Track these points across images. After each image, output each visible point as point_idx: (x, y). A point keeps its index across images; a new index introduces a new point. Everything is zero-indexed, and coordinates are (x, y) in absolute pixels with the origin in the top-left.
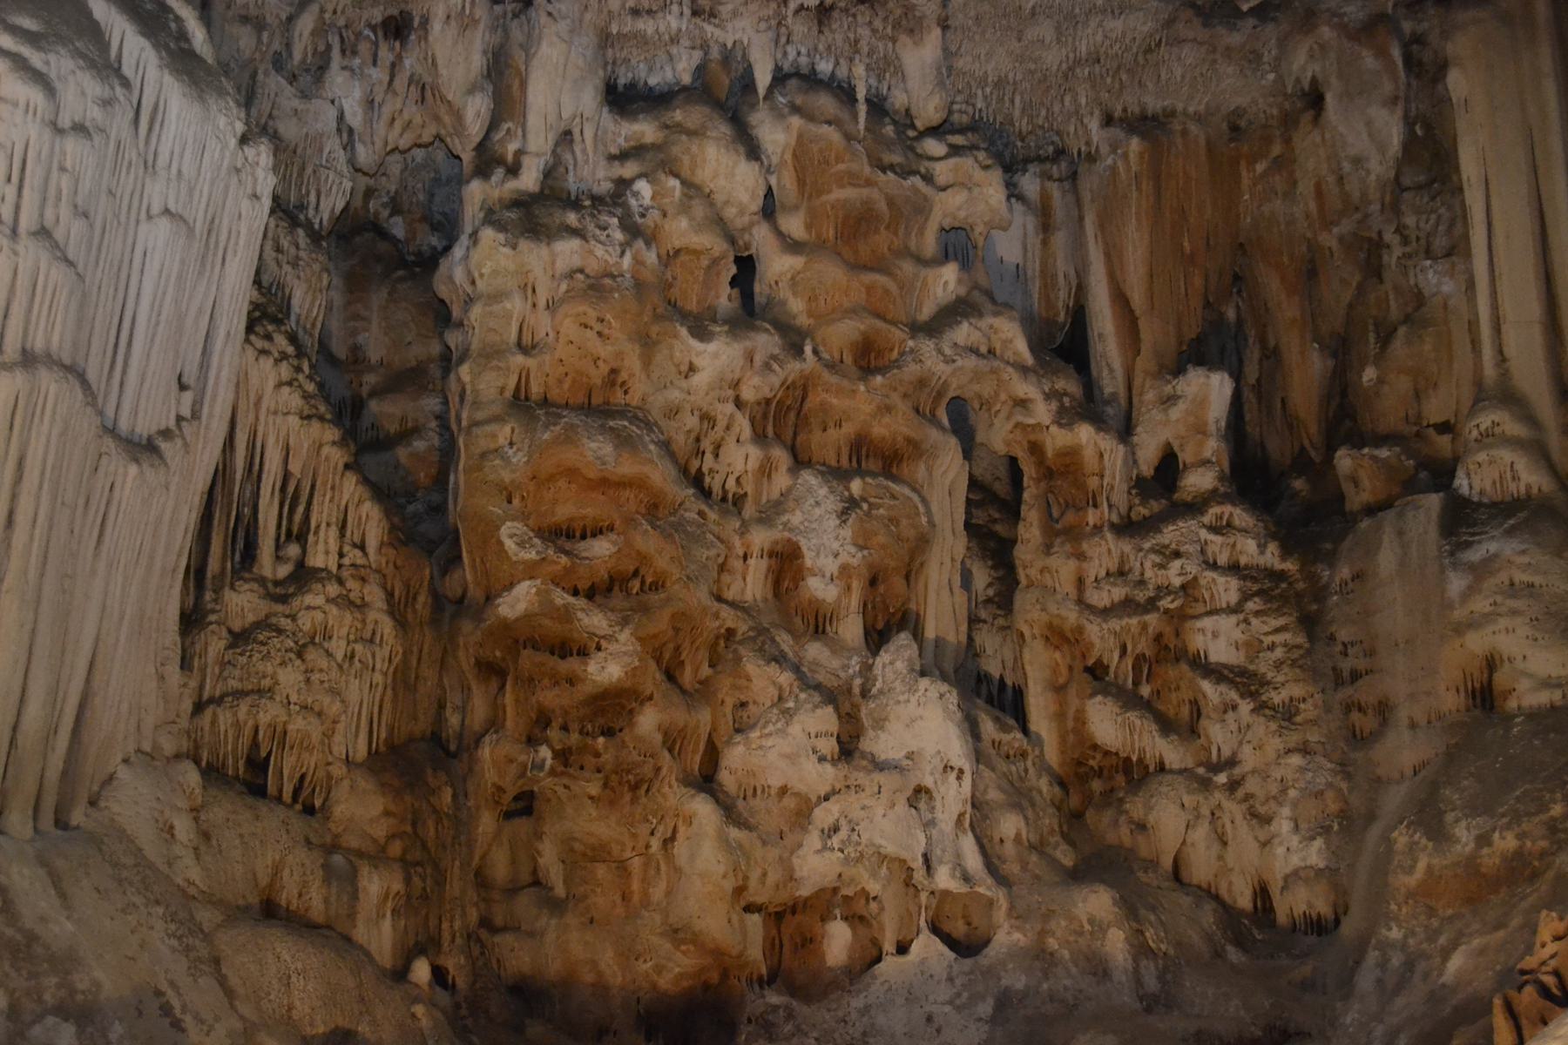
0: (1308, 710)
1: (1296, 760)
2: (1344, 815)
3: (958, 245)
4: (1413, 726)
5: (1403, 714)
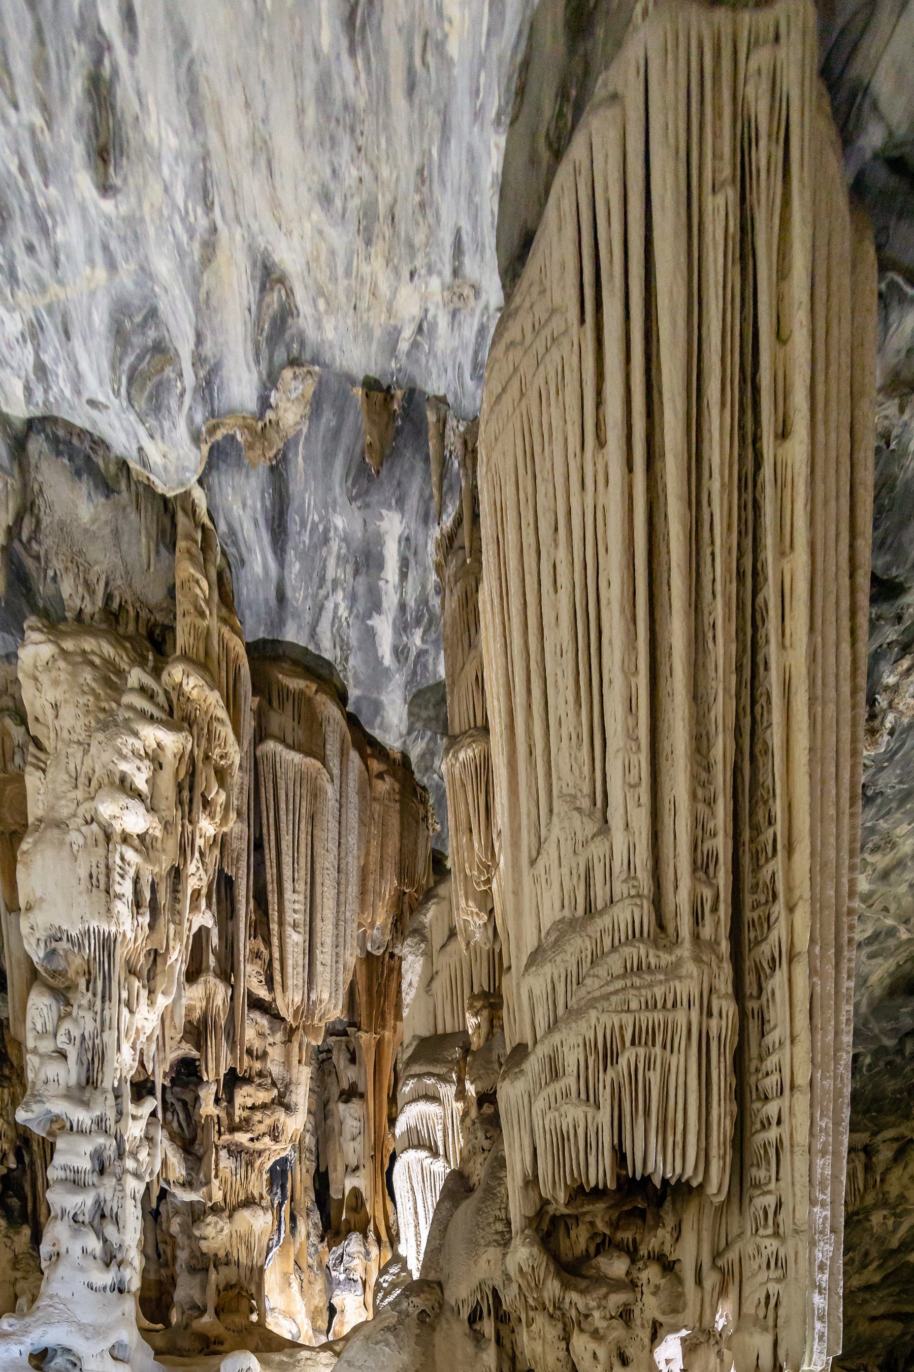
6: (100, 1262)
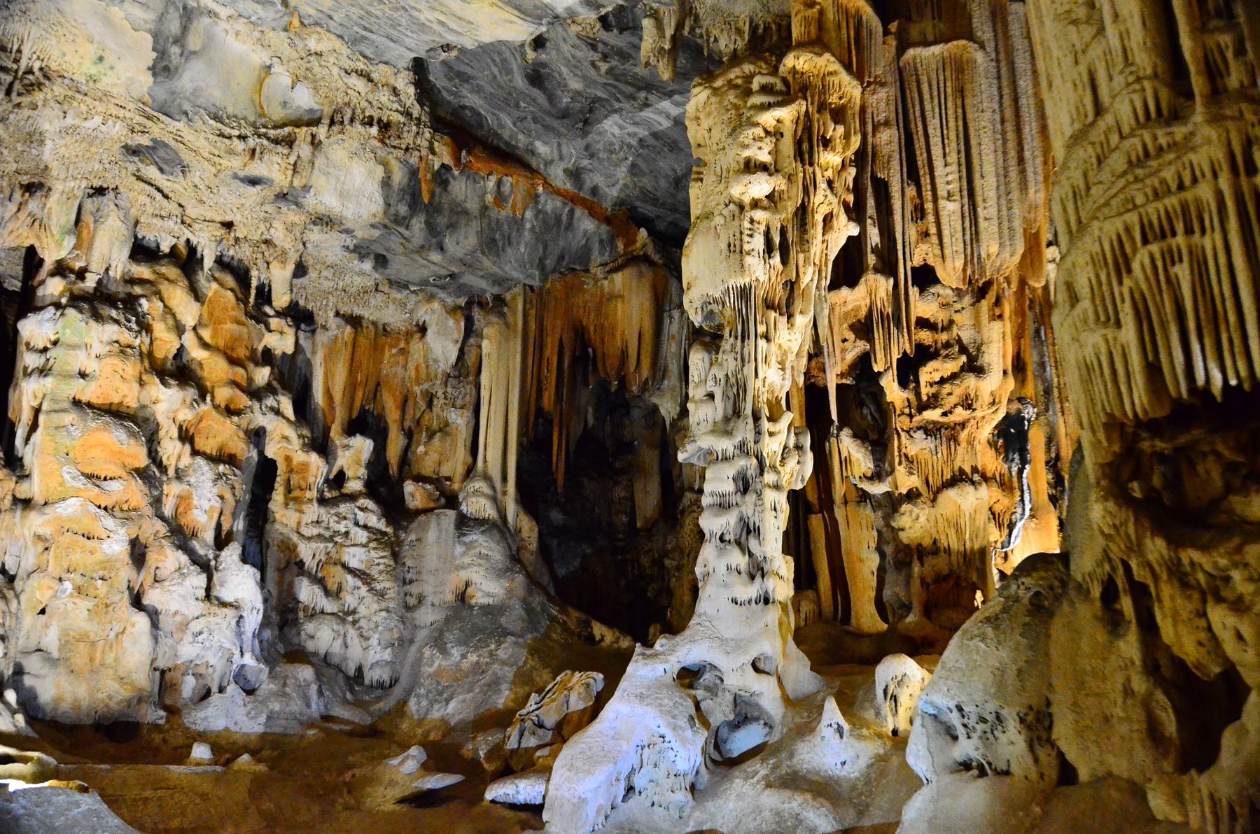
0: (391, 594)
1: (384, 614)
2: (401, 640)
3: (267, 357)
4: (433, 605)
5: (429, 599)
6: (744, 576)
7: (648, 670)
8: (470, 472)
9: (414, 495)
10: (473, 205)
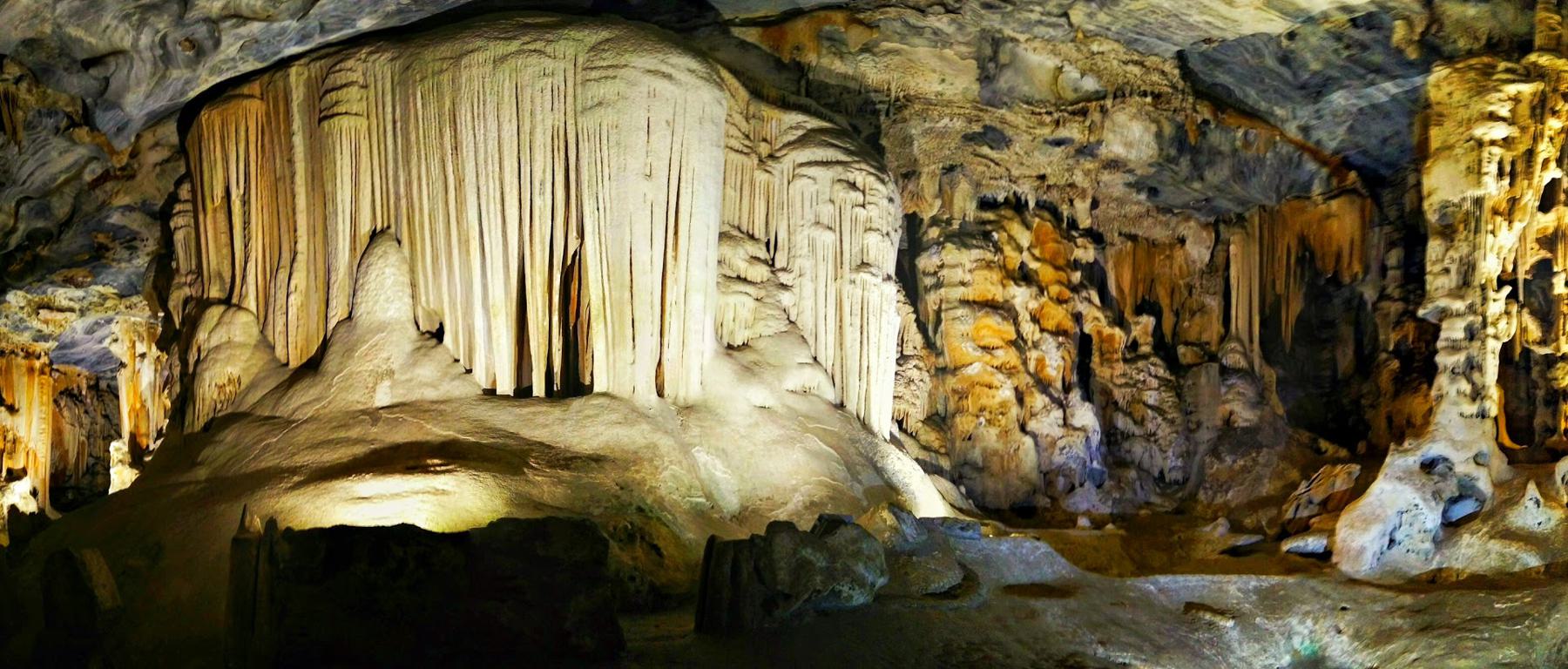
0: (1178, 421)
2: (1188, 452)
7: (1400, 461)
8: (1223, 339)
9: (1185, 354)
10: (1226, 148)
